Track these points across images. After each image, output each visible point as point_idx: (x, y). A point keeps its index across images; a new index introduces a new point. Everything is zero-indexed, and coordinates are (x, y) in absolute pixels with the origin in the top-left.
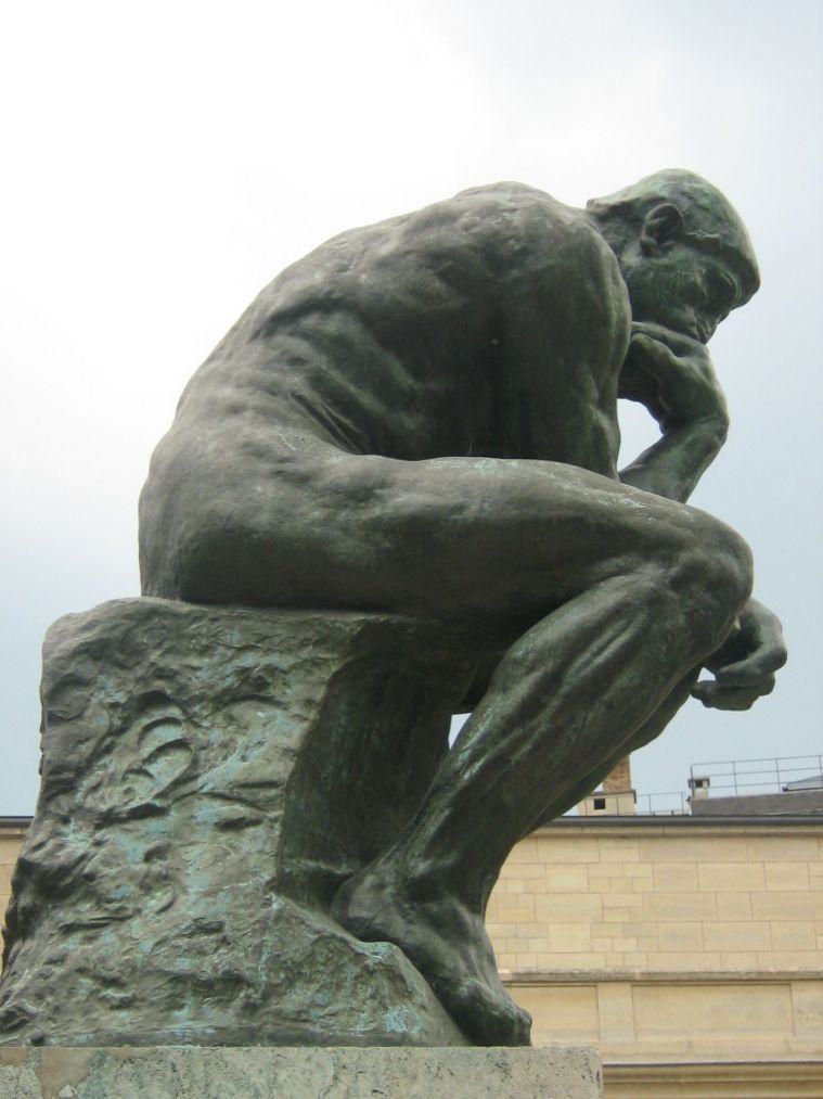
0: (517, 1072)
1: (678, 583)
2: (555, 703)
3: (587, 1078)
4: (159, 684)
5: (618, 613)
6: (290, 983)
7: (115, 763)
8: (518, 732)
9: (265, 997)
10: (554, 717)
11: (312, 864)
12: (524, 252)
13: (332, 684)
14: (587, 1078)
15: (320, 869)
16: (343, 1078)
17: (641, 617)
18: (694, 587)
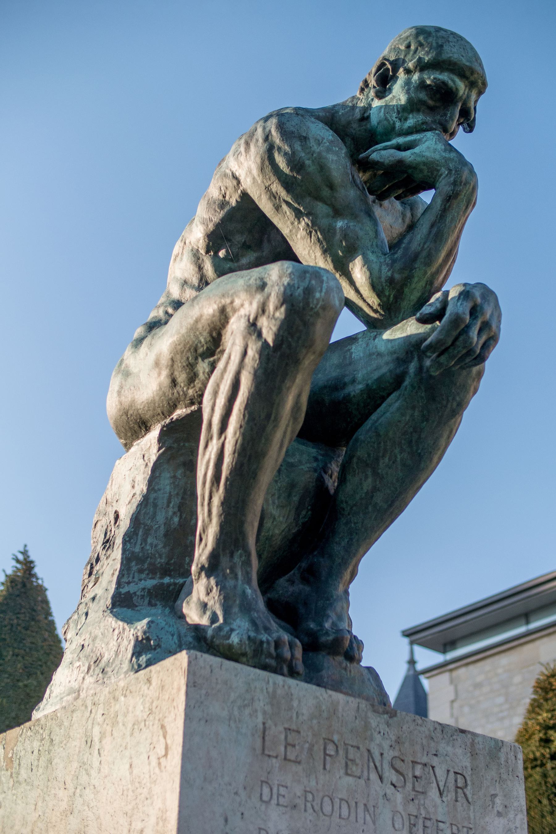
3: (181, 673)
14: (181, 673)
15: (163, 584)
16: (93, 711)
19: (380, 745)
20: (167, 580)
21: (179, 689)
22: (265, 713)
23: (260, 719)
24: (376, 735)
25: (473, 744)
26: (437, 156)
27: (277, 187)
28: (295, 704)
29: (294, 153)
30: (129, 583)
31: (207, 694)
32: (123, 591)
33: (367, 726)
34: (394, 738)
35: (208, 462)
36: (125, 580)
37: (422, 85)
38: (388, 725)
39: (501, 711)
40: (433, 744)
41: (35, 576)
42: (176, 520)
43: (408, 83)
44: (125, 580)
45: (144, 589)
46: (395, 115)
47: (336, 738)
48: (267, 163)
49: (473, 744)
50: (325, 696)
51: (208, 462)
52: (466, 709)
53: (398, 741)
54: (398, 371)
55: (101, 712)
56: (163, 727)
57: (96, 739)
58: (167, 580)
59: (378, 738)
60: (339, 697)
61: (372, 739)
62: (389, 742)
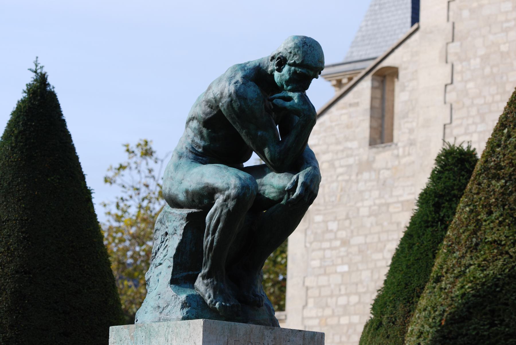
0: (191, 326)
1: (225, 200)
2: (211, 232)
4: (167, 230)
5: (216, 210)
6: (167, 306)
7: (161, 250)
8: (207, 240)
9: (163, 310)
10: (212, 236)
11: (185, 274)
12: (221, 98)
13: (185, 229)
17: (219, 210)
18: (229, 200)
19: (268, 341)
20: (190, 273)
21: (200, 332)
22: (228, 336)
23: (226, 338)
24: (266, 337)
25: (304, 335)
26: (299, 108)
27: (233, 115)
28: (238, 331)
29: (241, 105)
30: (176, 274)
31: (209, 333)
32: (174, 277)
33: (263, 335)
34: (273, 338)
35: (208, 242)
36: (175, 273)
37: (295, 72)
38: (271, 333)
39: (507, 21)
40: (288, 338)
41: (49, 84)
42: (194, 249)
43: (289, 70)
44: (175, 273)
45: (182, 277)
46: (284, 82)
47: (252, 341)
48: (230, 106)
49: (304, 335)
50: (249, 326)
51: (208, 242)
52: (466, 13)
53: (275, 339)
54: (281, 196)
55: (171, 330)
56: (195, 343)
57: (170, 340)
58: (190, 273)
59: (267, 338)
60: (254, 326)
61: (265, 339)
62: (271, 340)
